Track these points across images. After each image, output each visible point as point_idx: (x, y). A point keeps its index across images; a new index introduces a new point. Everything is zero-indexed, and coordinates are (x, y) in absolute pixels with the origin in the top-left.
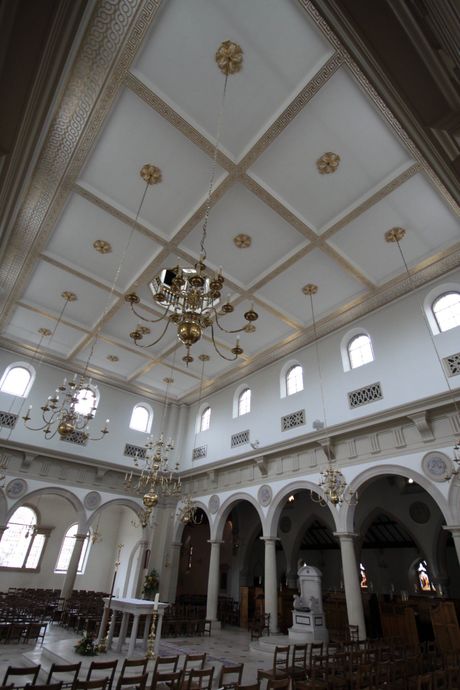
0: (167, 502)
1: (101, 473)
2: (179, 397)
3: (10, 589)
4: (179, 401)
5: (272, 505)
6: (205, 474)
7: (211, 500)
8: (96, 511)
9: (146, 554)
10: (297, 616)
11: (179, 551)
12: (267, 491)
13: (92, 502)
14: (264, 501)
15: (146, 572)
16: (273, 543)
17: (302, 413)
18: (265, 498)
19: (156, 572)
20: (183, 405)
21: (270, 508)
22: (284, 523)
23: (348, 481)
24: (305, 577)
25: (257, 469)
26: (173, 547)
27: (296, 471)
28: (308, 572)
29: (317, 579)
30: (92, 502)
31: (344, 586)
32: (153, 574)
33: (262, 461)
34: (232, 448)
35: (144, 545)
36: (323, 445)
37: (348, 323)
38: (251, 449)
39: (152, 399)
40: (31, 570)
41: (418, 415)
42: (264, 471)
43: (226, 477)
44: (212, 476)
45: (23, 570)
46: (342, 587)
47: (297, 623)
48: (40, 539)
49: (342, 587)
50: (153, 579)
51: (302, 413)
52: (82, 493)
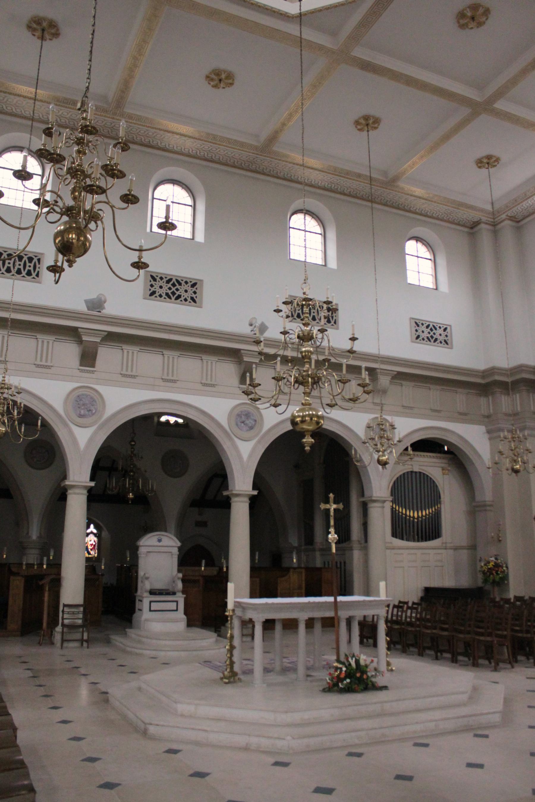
5: (100, 428)
10: (151, 602)
12: (94, 401)
14: (81, 416)
16: (85, 492)
18: (82, 412)
21: (95, 433)
23: (267, 426)
24: (150, 548)
25: (68, 352)
27: (170, 381)
28: (160, 541)
29: (176, 551)
33: (98, 340)
36: (246, 359)
37: (311, 186)
38: (82, 308)
41: (385, 372)
42: (88, 358)
47: (150, 610)
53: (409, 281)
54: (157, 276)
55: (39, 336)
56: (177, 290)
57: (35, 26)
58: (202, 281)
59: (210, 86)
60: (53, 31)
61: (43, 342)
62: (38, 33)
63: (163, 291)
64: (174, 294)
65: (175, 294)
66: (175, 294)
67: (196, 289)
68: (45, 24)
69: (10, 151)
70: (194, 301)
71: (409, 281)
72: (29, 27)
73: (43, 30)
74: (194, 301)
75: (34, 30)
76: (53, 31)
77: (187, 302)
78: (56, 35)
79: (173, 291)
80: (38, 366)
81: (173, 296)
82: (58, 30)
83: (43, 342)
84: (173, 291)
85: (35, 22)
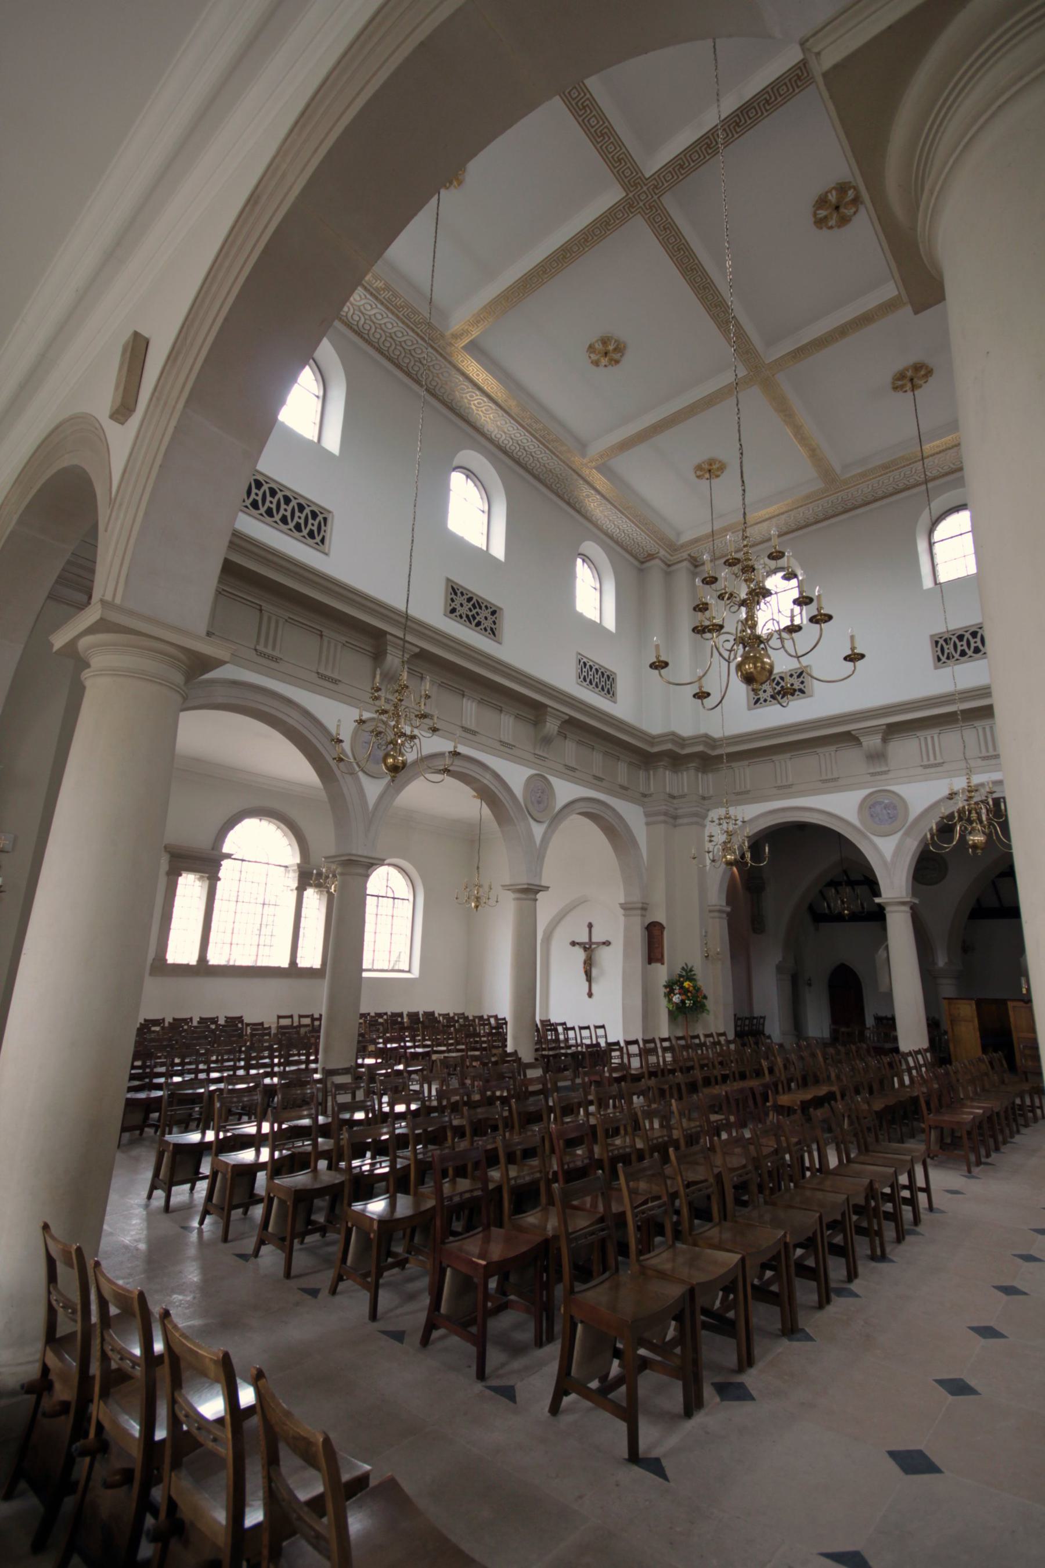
0: (680, 812)
1: (552, 726)
2: (685, 538)
3: (279, 1017)
4: (673, 547)
6: (849, 738)
7: (868, 806)
8: (549, 826)
9: (654, 934)
11: (725, 923)
13: (539, 802)
15: (662, 973)
19: (691, 970)
20: (685, 564)
22: (928, 867)
26: (716, 914)
30: (539, 802)
31: (1029, 990)
32: (688, 974)
34: (936, 668)
35: (639, 912)
39: (611, 537)
40: (310, 972)
43: (905, 749)
44: (872, 742)
45: (293, 971)
46: (1024, 991)
48: (315, 903)
49: (1024, 991)
50: (694, 987)
52: (516, 775)
53: (972, 570)
55: (919, 734)
57: (900, 383)
60: (923, 372)
61: (984, 729)
68: (909, 374)
69: (944, 519)
71: (972, 570)
72: (895, 388)
73: (912, 380)
75: (902, 387)
76: (923, 372)
78: (929, 372)
80: (926, 767)
82: (927, 367)
83: (984, 729)
85: (899, 379)
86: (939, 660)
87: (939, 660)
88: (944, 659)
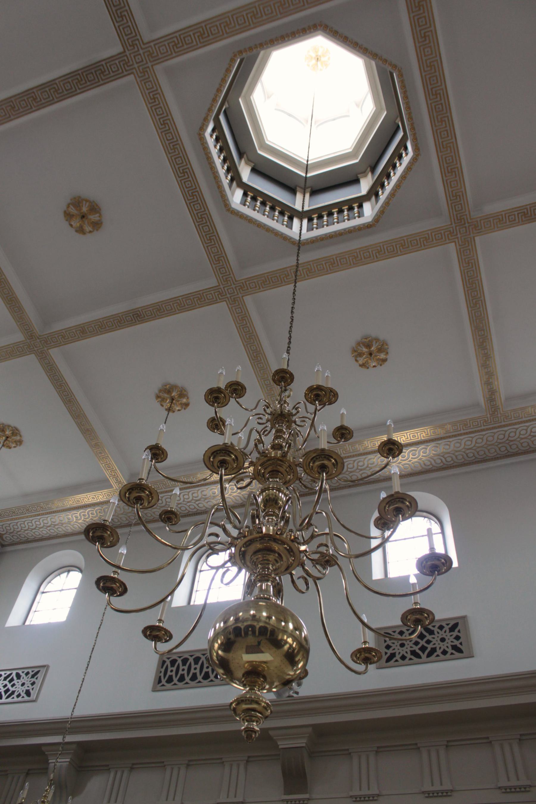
17: (456, 625)
34: (154, 690)
51: (456, 625)
54: (394, 632)
56: (428, 642)
58: (464, 618)
59: (357, 364)
62: (167, 404)
63: (406, 650)
64: (423, 649)
65: (427, 648)
66: (427, 648)
67: (459, 631)
70: (460, 651)
74: (460, 651)
77: (448, 656)
79: (423, 646)
81: (424, 653)
84: (423, 646)
86: (160, 681)
87: (160, 681)
88: (164, 681)
